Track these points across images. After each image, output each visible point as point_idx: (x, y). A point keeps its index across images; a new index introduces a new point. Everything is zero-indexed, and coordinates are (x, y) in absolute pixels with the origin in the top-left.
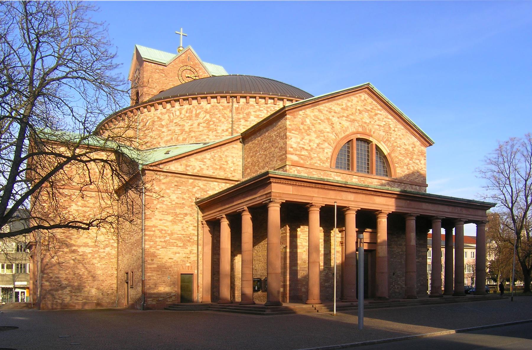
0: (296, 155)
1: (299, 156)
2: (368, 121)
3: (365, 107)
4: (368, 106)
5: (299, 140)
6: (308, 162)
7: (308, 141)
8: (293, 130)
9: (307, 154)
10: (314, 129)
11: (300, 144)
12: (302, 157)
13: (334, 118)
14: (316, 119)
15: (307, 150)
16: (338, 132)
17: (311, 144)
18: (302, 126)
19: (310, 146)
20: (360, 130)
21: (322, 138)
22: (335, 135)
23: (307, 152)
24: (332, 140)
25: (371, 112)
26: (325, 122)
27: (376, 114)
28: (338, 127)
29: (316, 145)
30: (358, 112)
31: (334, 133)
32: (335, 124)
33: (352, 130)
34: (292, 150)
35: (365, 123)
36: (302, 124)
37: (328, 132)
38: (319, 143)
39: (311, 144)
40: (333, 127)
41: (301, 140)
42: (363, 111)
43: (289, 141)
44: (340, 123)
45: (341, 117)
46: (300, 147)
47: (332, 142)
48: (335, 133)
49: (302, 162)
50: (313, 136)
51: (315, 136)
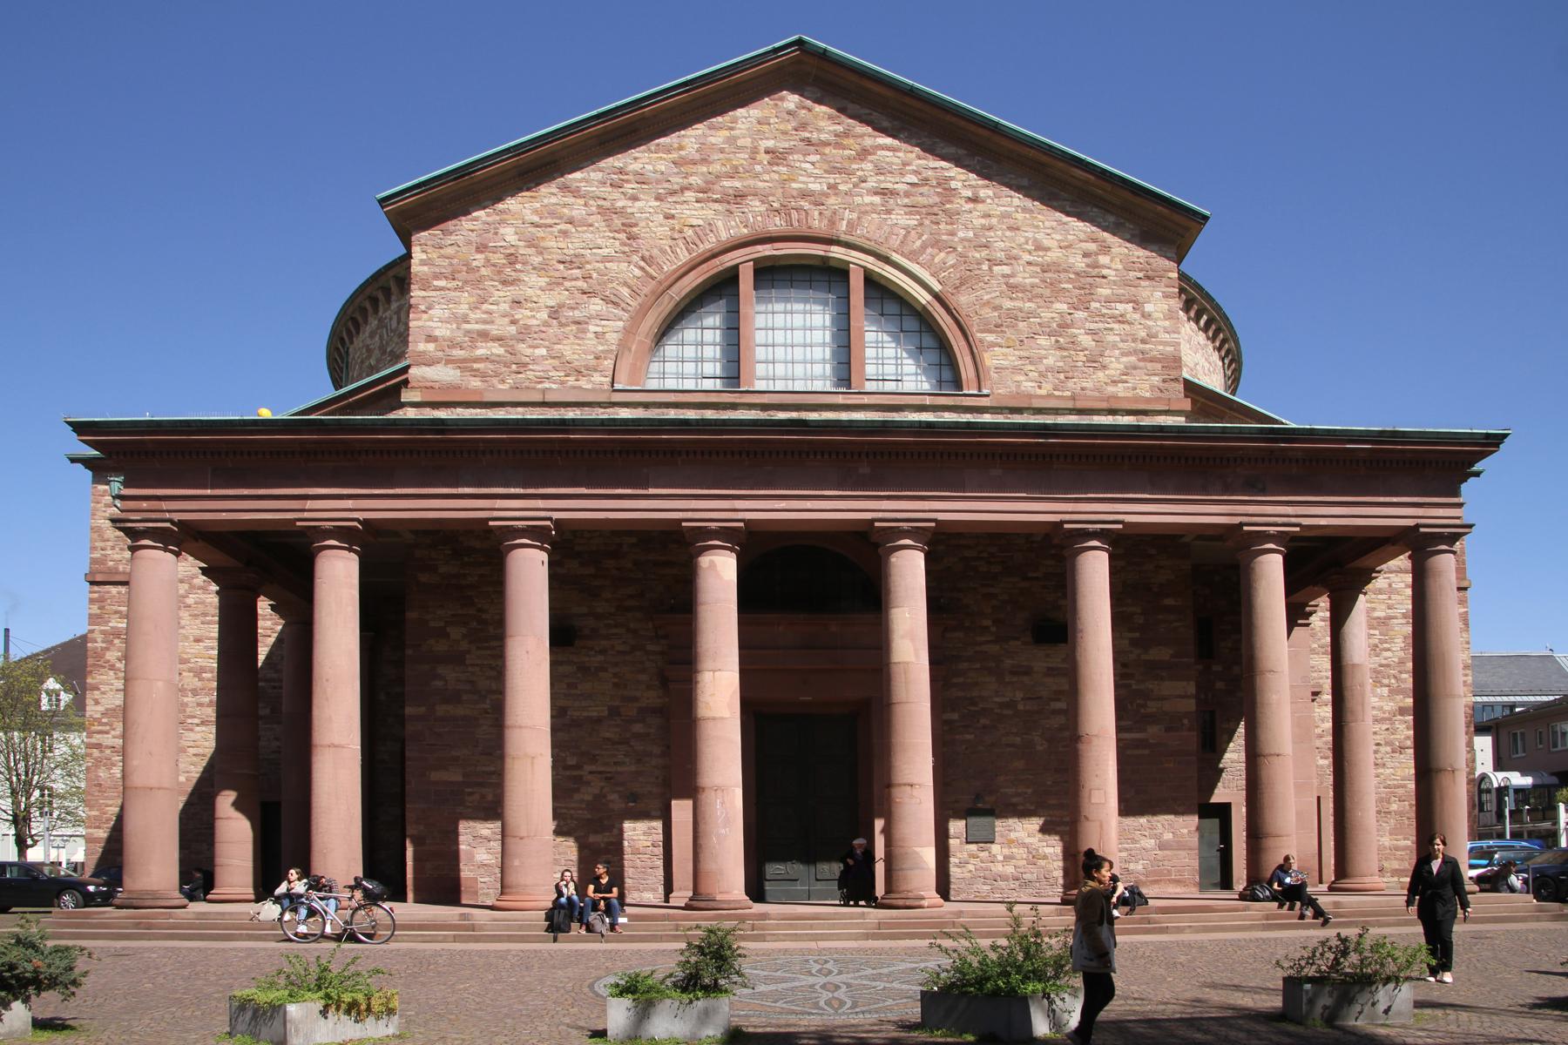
0: (448, 362)
1: (463, 365)
2: (815, 187)
3: (807, 135)
4: (819, 130)
5: (463, 309)
6: (503, 381)
7: (505, 307)
8: (437, 277)
9: (501, 351)
10: (537, 260)
11: (468, 322)
12: (476, 366)
13: (638, 204)
14: (549, 221)
15: (499, 339)
16: (655, 252)
17: (520, 314)
18: (478, 256)
19: (513, 322)
20: (777, 225)
21: (573, 283)
22: (642, 264)
23: (501, 346)
24: (626, 284)
25: (838, 146)
26: (591, 225)
27: (864, 154)
28: (654, 231)
29: (544, 315)
30: (765, 158)
31: (635, 258)
32: (642, 224)
33: (728, 229)
34: (431, 347)
35: (804, 195)
36: (481, 248)
37: (606, 259)
38: (561, 306)
39: (520, 314)
40: (631, 237)
41: (473, 308)
42: (791, 151)
43: (419, 319)
44: (669, 217)
45: (673, 193)
46: (468, 332)
47: (625, 291)
48: (643, 258)
49: (476, 383)
50: (533, 283)
51: (543, 282)
